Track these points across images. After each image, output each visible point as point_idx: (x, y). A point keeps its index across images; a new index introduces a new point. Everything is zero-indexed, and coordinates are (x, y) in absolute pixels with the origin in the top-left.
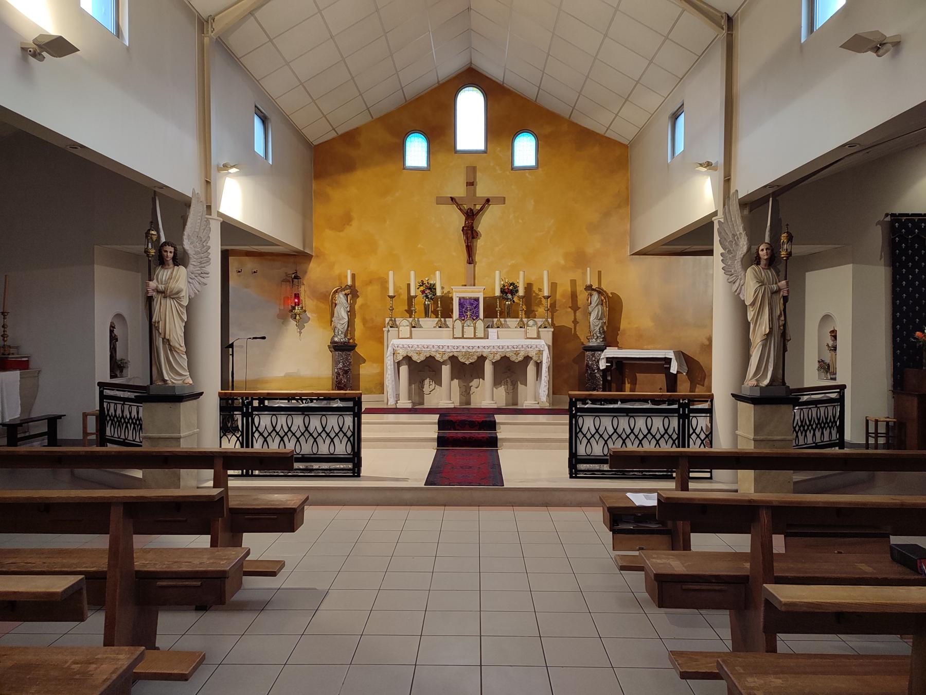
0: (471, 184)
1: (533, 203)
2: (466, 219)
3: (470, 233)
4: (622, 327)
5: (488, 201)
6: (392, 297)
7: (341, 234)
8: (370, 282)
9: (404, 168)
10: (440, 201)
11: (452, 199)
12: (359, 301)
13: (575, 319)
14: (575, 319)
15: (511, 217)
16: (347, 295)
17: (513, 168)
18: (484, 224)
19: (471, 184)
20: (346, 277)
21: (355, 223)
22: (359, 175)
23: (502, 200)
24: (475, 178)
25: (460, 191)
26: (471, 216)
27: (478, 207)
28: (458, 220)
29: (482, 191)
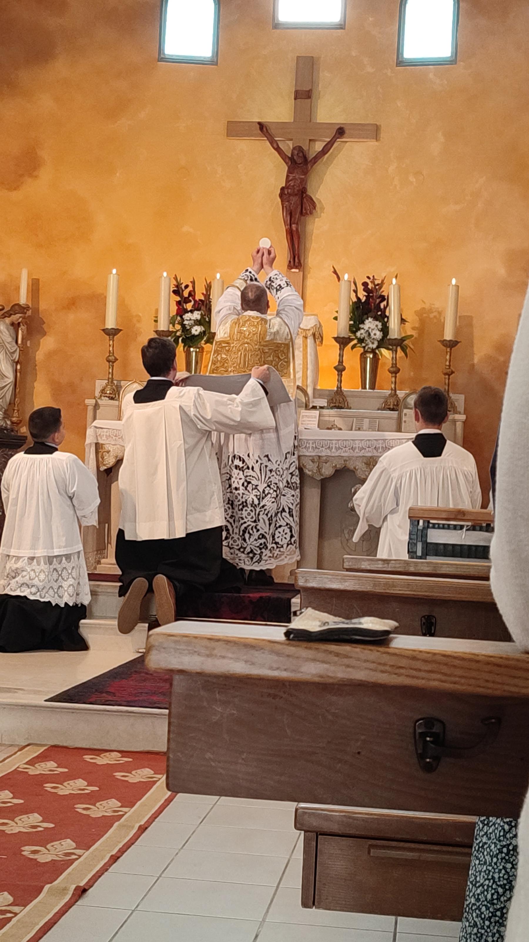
0: (304, 95)
1: (442, 139)
2: (289, 172)
3: (297, 204)
4: (40, 309)
5: (341, 132)
6: (112, 333)
7: (15, 195)
8: (72, 304)
9: (161, 58)
10: (235, 129)
11: (261, 126)
12: (47, 344)
13: (341, 362)
14: (341, 362)
15: (392, 168)
16: (15, 326)
17: (401, 62)
18: (328, 186)
19: (304, 95)
20: (18, 289)
21: (45, 174)
22: (60, 68)
23: (374, 132)
24: (313, 82)
25: (279, 110)
26: (301, 164)
27: (319, 146)
28: (273, 173)
29: (329, 111)
